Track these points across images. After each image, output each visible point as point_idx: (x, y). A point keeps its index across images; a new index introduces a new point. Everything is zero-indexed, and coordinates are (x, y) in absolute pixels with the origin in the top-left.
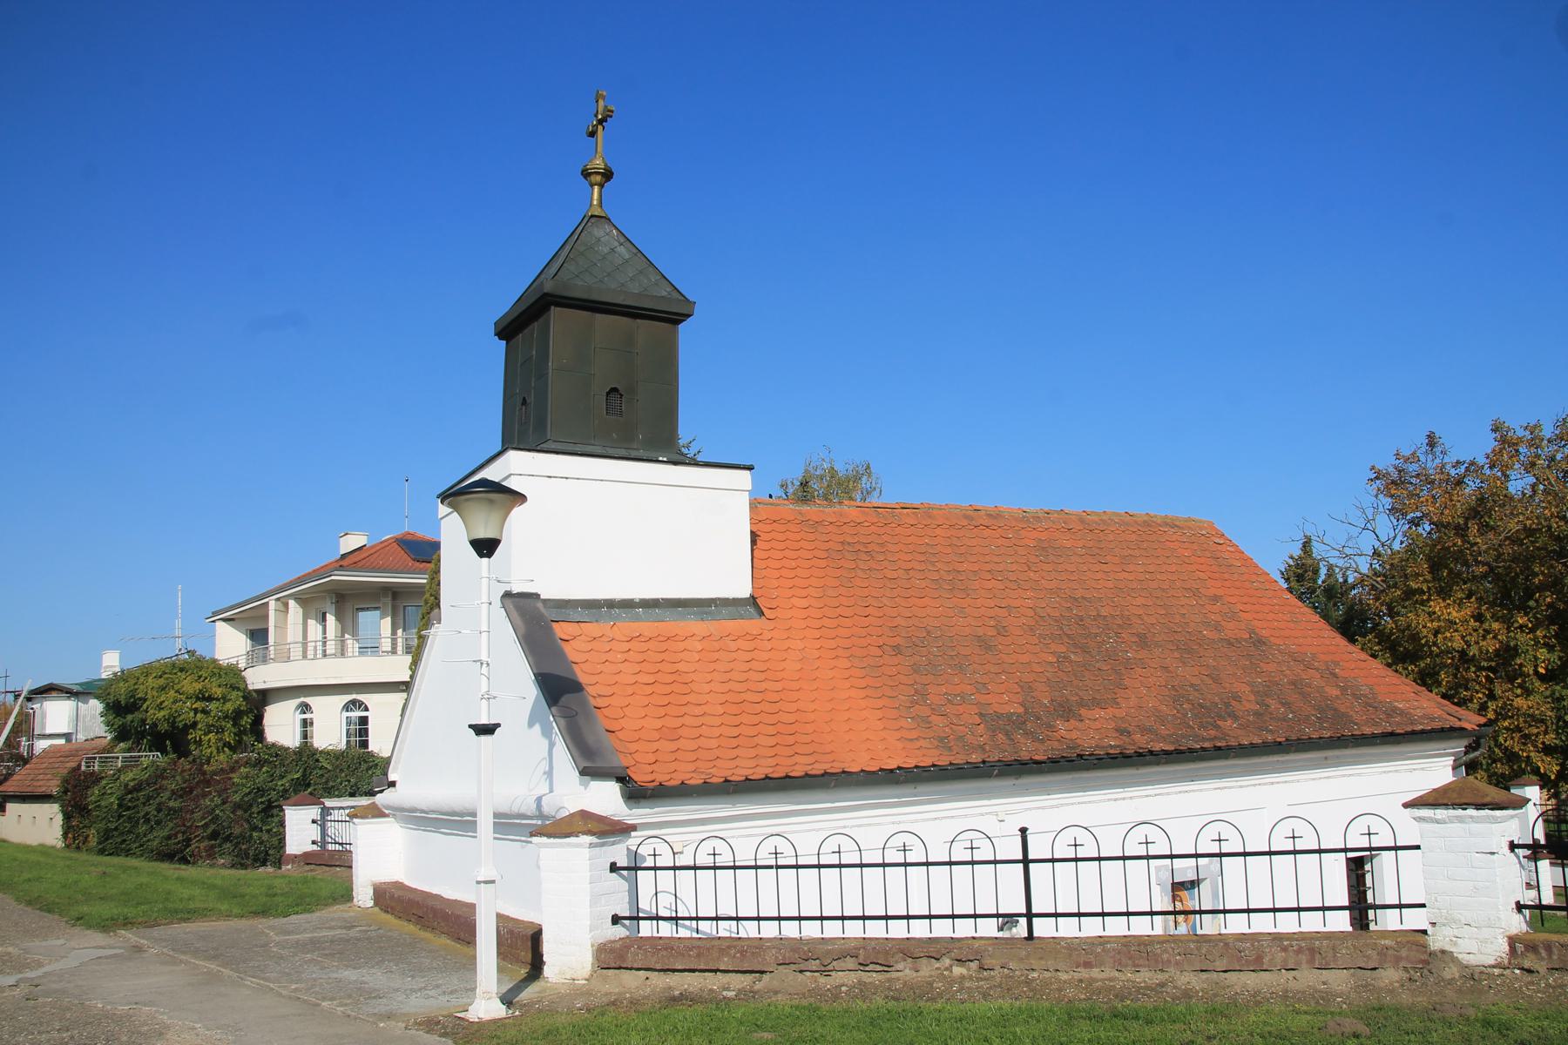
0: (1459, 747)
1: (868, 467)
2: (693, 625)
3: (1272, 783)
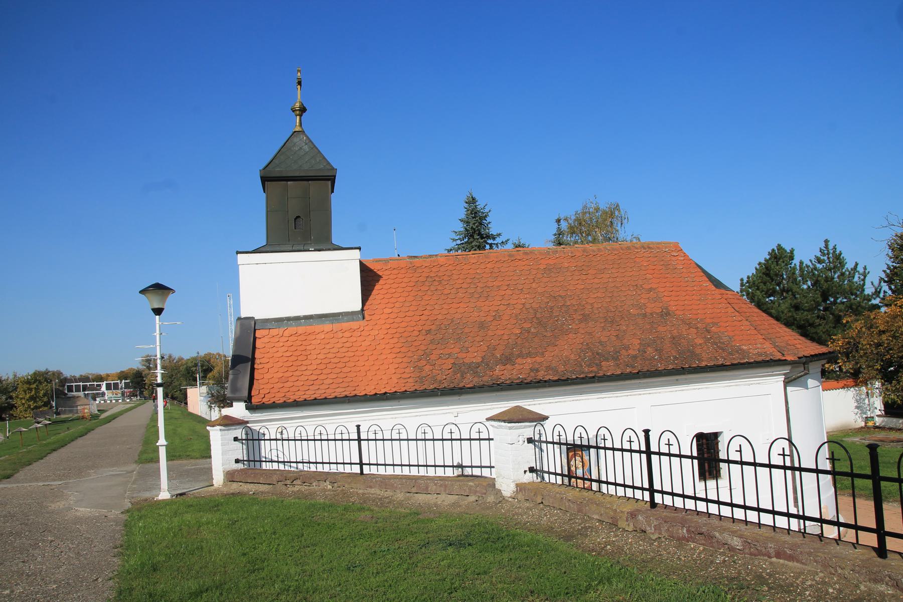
0: (787, 370)
1: (618, 205)
2: (327, 326)
3: (640, 394)
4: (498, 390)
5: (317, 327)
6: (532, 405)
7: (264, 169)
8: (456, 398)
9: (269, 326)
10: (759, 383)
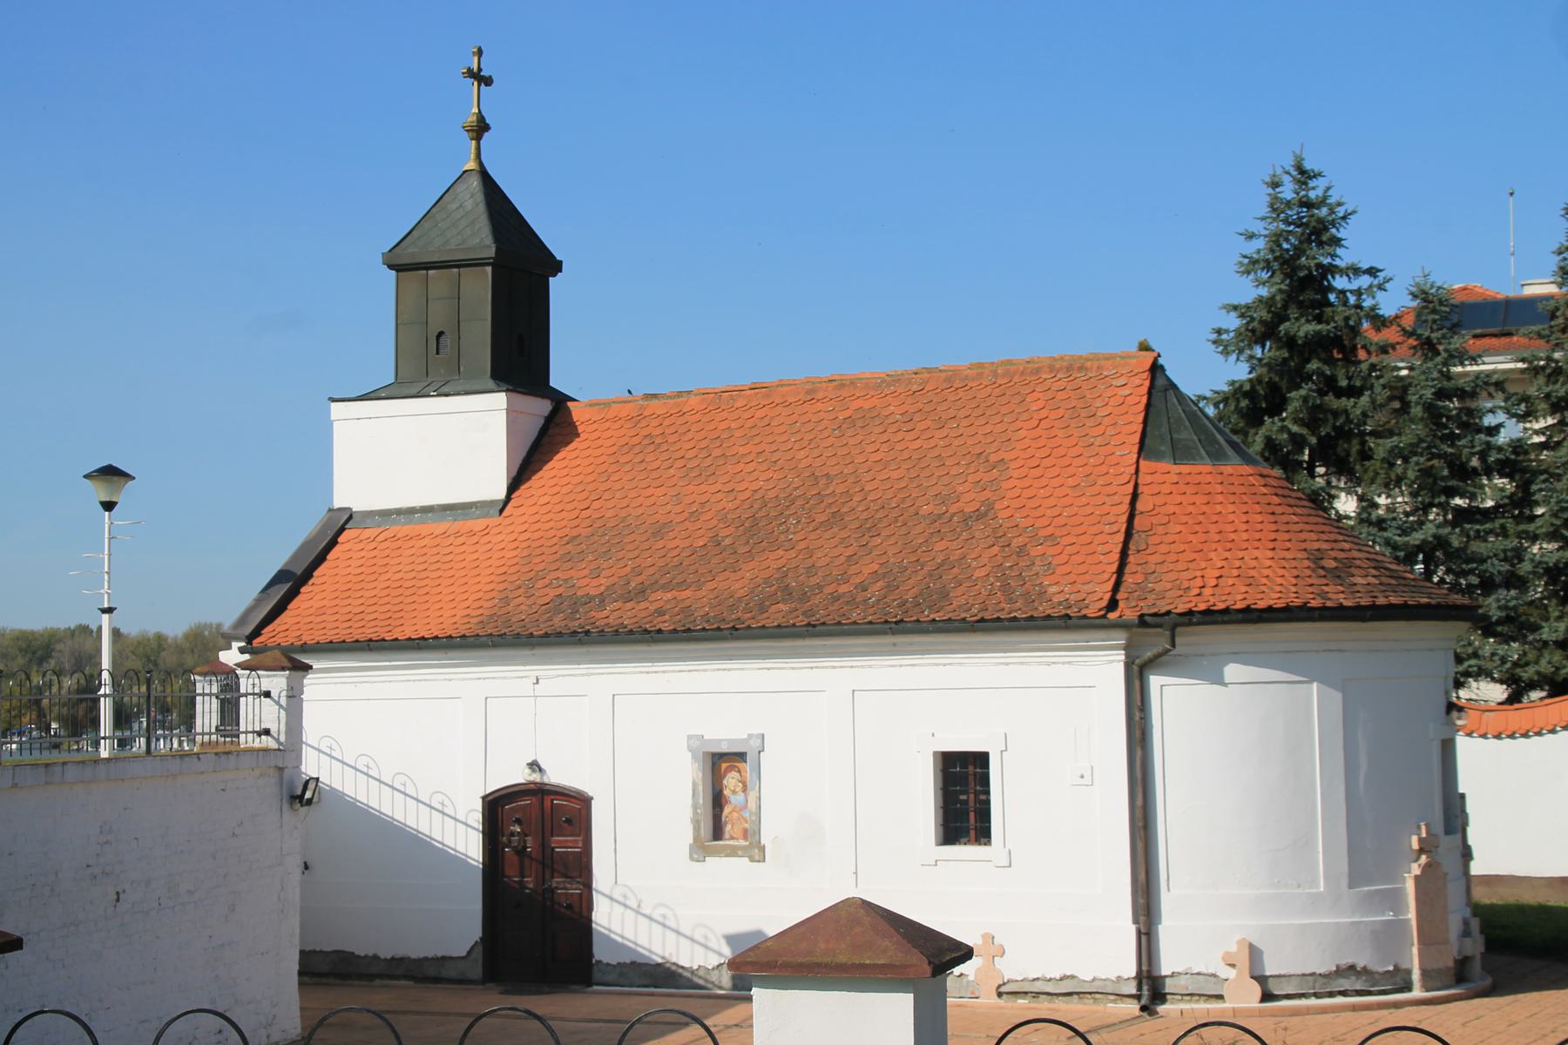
0: (1120, 638)
4: (581, 643)
5: (403, 529)
6: (652, 672)
7: (390, 251)
8: (526, 652)
9: (369, 523)
10: (1069, 663)
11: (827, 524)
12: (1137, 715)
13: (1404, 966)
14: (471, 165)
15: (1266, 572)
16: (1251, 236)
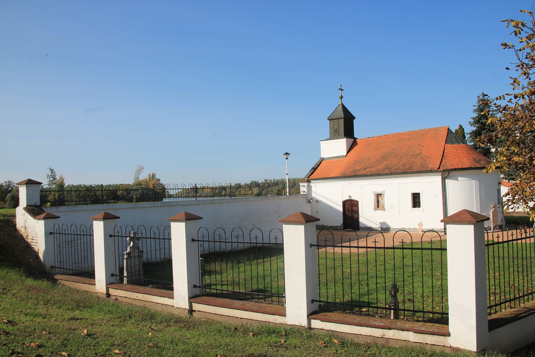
0: (440, 174)
4: (356, 177)
5: (331, 160)
8: (348, 179)
9: (326, 159)
11: (395, 157)
12: (444, 186)
13: (490, 226)
14: (340, 103)
15: (465, 162)
16: (475, 106)
